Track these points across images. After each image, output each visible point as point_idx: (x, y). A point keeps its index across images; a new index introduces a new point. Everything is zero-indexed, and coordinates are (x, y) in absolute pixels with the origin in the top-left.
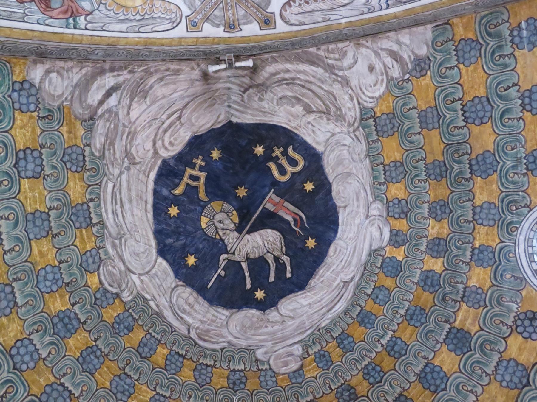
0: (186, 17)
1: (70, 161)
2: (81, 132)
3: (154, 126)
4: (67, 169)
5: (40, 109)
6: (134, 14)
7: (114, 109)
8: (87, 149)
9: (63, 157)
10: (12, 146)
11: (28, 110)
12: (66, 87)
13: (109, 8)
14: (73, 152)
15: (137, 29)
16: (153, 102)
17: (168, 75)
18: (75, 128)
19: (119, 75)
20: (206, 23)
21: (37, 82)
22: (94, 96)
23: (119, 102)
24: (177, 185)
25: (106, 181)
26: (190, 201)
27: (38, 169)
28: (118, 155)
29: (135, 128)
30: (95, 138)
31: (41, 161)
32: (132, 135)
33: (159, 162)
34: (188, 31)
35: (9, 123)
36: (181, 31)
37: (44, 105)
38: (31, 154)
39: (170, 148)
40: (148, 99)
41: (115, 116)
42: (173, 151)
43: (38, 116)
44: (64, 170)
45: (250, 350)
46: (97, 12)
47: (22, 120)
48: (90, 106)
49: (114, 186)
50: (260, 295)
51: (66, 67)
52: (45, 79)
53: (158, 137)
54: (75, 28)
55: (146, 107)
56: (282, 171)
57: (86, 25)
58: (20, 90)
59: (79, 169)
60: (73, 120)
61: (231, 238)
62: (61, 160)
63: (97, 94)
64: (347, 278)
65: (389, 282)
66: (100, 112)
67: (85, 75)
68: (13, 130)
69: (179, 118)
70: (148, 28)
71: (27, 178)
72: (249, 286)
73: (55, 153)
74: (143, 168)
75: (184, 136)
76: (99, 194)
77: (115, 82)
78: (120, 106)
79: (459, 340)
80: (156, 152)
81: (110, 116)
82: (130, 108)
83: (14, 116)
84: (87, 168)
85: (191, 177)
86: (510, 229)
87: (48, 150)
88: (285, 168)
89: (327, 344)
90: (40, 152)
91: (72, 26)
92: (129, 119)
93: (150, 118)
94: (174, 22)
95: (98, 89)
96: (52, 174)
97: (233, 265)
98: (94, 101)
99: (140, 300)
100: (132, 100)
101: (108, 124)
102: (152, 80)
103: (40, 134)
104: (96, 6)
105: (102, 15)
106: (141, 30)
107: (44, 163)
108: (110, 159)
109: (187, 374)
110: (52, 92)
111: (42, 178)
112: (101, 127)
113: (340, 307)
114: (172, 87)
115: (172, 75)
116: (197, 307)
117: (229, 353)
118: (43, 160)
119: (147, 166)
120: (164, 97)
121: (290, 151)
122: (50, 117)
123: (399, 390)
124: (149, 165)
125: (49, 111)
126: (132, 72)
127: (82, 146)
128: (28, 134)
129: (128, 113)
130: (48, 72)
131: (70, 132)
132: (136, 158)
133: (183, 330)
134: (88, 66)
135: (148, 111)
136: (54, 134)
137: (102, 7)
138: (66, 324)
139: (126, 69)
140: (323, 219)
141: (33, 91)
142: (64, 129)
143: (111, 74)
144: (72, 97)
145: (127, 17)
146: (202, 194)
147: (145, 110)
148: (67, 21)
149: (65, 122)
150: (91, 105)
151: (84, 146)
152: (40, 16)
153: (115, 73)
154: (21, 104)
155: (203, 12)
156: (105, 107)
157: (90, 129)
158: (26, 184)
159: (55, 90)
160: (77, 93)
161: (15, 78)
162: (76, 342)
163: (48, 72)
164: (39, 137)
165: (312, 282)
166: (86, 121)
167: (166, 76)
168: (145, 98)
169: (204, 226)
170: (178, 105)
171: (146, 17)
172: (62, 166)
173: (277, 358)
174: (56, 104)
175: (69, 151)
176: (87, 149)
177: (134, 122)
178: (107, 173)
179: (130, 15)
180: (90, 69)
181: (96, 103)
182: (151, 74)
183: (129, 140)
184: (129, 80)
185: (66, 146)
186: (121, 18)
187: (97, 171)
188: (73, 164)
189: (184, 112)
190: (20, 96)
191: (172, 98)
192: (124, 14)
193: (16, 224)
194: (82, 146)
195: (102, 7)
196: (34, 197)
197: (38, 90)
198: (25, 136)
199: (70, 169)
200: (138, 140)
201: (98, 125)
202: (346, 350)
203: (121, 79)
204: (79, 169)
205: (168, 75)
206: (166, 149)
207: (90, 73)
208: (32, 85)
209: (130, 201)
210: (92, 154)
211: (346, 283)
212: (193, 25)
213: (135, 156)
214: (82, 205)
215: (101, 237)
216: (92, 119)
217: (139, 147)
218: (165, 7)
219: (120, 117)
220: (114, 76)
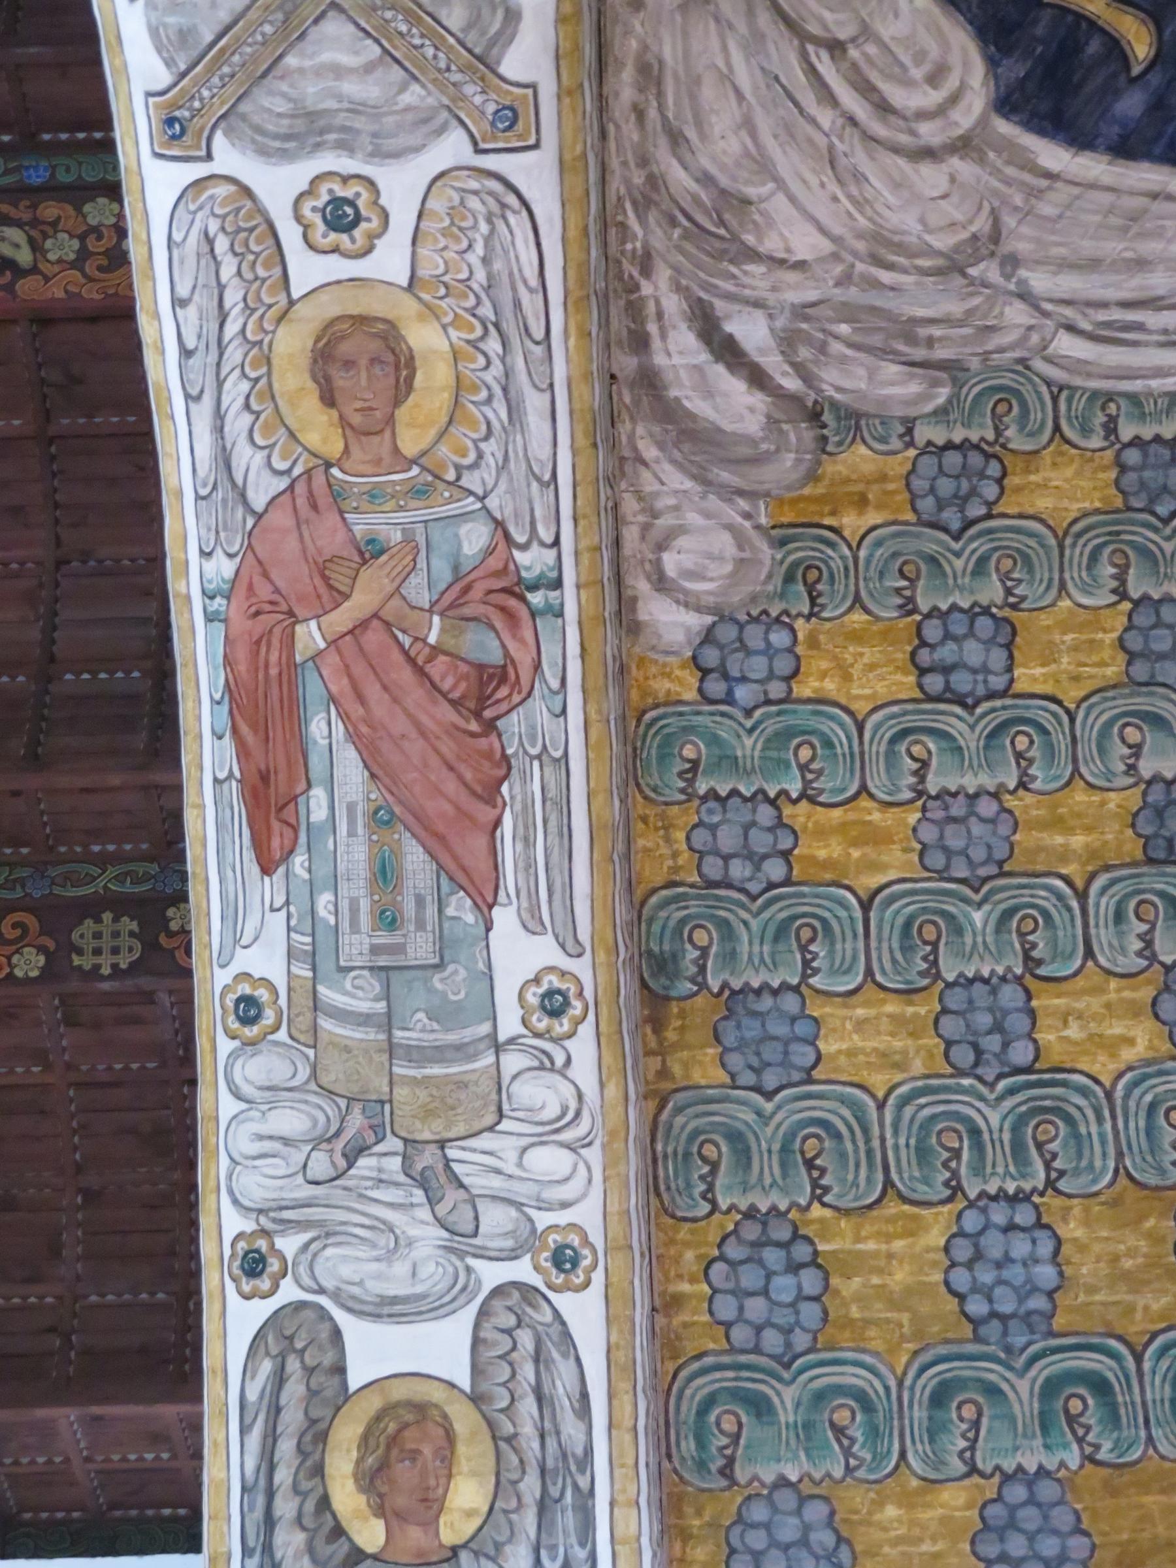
0: (479, 151)
1: (961, 500)
2: (859, 459)
3: (861, 159)
4: (989, 516)
5: (786, 612)
6: (482, 361)
7: (780, 323)
8: (924, 433)
9: (946, 530)
10: (905, 713)
11: (790, 651)
12: (707, 515)
13: (472, 457)
14: (932, 490)
15: (538, 351)
16: (764, 168)
17: (661, 108)
18: (847, 481)
19: (660, 315)
20: (504, 69)
21: (696, 621)
22: (735, 406)
23: (758, 304)
24: (1116, 49)
25: (1049, 360)
27: (984, 623)
28: (956, 308)
29: (860, 236)
30: (885, 401)
31: (956, 616)
32: (884, 248)
33: (1004, 127)
34: (536, 146)
35: (832, 718)
36: (535, 174)
37: (770, 598)
38: (932, 647)
39: (952, 83)
40: (751, 192)
41: (807, 319)
42: (966, 64)
43: (808, 618)
44: (990, 531)
46: (493, 502)
47: (823, 675)
48: (772, 422)
49: (1071, 328)
51: (641, 518)
52: (686, 592)
53: (904, 139)
54: (558, 584)
55: (781, 198)
57: (542, 544)
58: (726, 676)
59: (994, 469)
60: (820, 490)
62: (957, 537)
63: (726, 395)
66: (791, 384)
67: (661, 446)
68: (854, 706)
69: (836, 48)
70: (531, 304)
71: (1010, 669)
73: (932, 560)
74: (1018, 200)
76: (1095, 394)
77: (683, 326)
78: (772, 299)
80: (963, 146)
81: (809, 341)
82: (782, 262)
83: (809, 701)
84: (990, 436)
87: (921, 583)
90: (928, 616)
91: (553, 595)
92: (821, 260)
93: (828, 177)
94: (504, 206)
95: (709, 393)
96: (1005, 577)
98: (752, 410)
100: (754, 256)
101: (836, 347)
102: (679, 178)
103: (867, 611)
104: (471, 504)
105: (503, 486)
106: (539, 334)
107: (965, 605)
108: (965, 341)
110: (728, 568)
111: (1014, 615)
112: (848, 378)
114: (708, 92)
115: (660, 95)
118: (954, 607)
119: (1008, 182)
120: (748, 125)
122: (813, 575)
124: (1011, 171)
125: (789, 578)
126: (646, 264)
127: (912, 453)
128: (870, 654)
129: (801, 265)
130: (661, 583)
131: (862, 502)
132: (973, 229)
134: (631, 437)
135: (795, 187)
136: (868, 561)
137: (471, 481)
139: (637, 288)
141: (728, 633)
142: (851, 522)
143: (656, 343)
144: (741, 493)
145: (498, 391)
147: (792, 199)
148: (543, 613)
149: (827, 521)
150: (769, 417)
151: (911, 444)
152: (539, 708)
153: (652, 328)
154: (771, 676)
155: (456, 77)
156: (772, 362)
157: (856, 421)
158: (1030, 676)
159: (721, 559)
160: (725, 476)
161: (691, 695)
163: (661, 583)
164: (877, 618)
166: (825, 439)
167: (664, 117)
168: (746, 202)
170: (784, 56)
171: (486, 311)
172: (979, 535)
174: (766, 552)
175: (927, 504)
176: (924, 433)
177: (836, 240)
178: (1017, 354)
179: (488, 377)
180: (640, 430)
181: (759, 400)
182: (654, 181)
183: (902, 260)
184: (677, 270)
185: (910, 516)
186: (504, 415)
187: (1006, 396)
188: (974, 492)
189: (813, 28)
190: (744, 679)
191: (756, 88)
192: (489, 400)
193: (1157, 721)
194: (912, 453)
195: (471, 481)
196: (1075, 648)
197: (723, 616)
198: (872, 667)
199: (990, 505)
200: (904, 221)
201: (839, 389)
203: (672, 304)
204: (994, 469)
205: (661, 108)
206: (954, 99)
207: (657, 429)
208: (708, 637)
209: (1141, 264)
210: (941, 414)
212: (511, 122)
213: (965, 235)
214: (1123, 468)
216: (815, 416)
217: (934, 220)
218: (445, 232)
219: (812, 295)
220: (663, 336)
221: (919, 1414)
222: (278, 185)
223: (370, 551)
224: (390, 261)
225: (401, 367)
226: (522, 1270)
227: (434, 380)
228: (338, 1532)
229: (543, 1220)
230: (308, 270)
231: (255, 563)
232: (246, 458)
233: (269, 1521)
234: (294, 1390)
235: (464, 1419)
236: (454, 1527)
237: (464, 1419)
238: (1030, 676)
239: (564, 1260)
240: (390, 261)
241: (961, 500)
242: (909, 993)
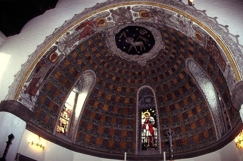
26: (123, 38)
32: (109, 33)
33: (115, 34)
45: (137, 62)
50: (139, 52)
56: (143, 33)
61: (132, 43)
64: (157, 52)
65: (164, 55)
72: (136, 51)
75: (120, 30)
79: (173, 70)
80: (114, 34)
85: (122, 35)
86: (185, 58)
88: (142, 33)
89: (150, 62)
97: (133, 48)
99: (115, 56)
109: (125, 65)
113: (155, 57)
116: (126, 55)
117: (133, 62)
121: (144, 30)
123: (162, 73)
133: (124, 58)
138: (104, 63)
140: (152, 41)
146: (125, 37)
158: (93, 49)
162: (106, 65)
165: (150, 52)
169: (126, 41)
173: (142, 63)
202: (154, 64)
209: (111, 42)
211: (156, 53)
215: (107, 49)
221: (62, 70)
222: (110, 16)
223: (93, 26)
224: (108, 21)
225: (103, 23)
226: (64, 54)
227: (103, 25)
228: (49, 57)
229: (67, 53)
230: (106, 18)
231: (90, 21)
232: (95, 19)
233: (48, 54)
234: (53, 50)
235: (57, 58)
236: (53, 61)
237: (57, 58)
238: (93, 49)
239: (66, 55)
240: (108, 21)
241: (99, 41)
242: (77, 54)
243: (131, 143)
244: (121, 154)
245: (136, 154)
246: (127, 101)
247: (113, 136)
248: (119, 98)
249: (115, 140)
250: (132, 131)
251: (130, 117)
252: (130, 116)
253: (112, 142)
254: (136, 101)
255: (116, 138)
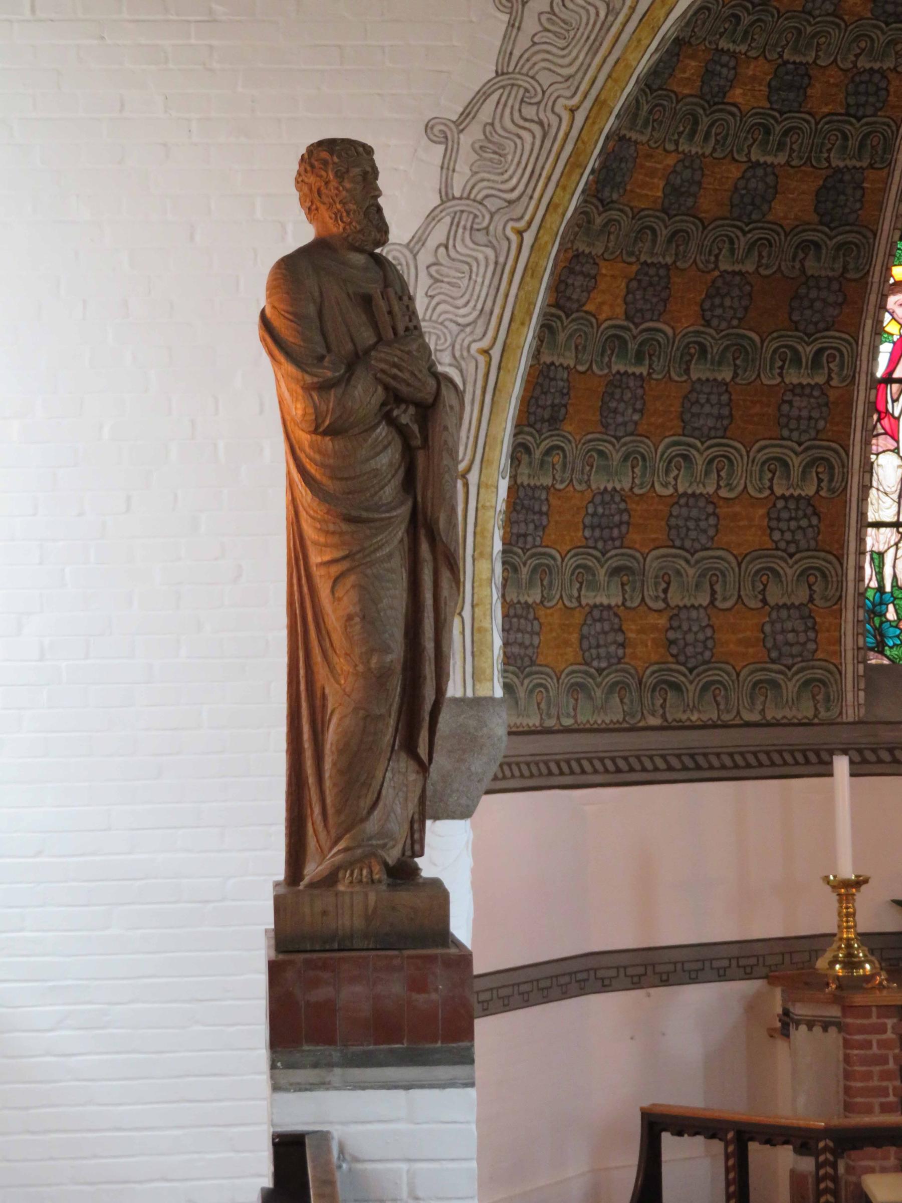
243: (806, 613)
244: (725, 726)
245: (850, 715)
246: (794, 204)
247: (653, 565)
248: (735, 172)
249: (675, 598)
250: (808, 500)
251: (797, 360)
252: (807, 351)
253: (653, 619)
254: (880, 206)
255: (678, 573)
